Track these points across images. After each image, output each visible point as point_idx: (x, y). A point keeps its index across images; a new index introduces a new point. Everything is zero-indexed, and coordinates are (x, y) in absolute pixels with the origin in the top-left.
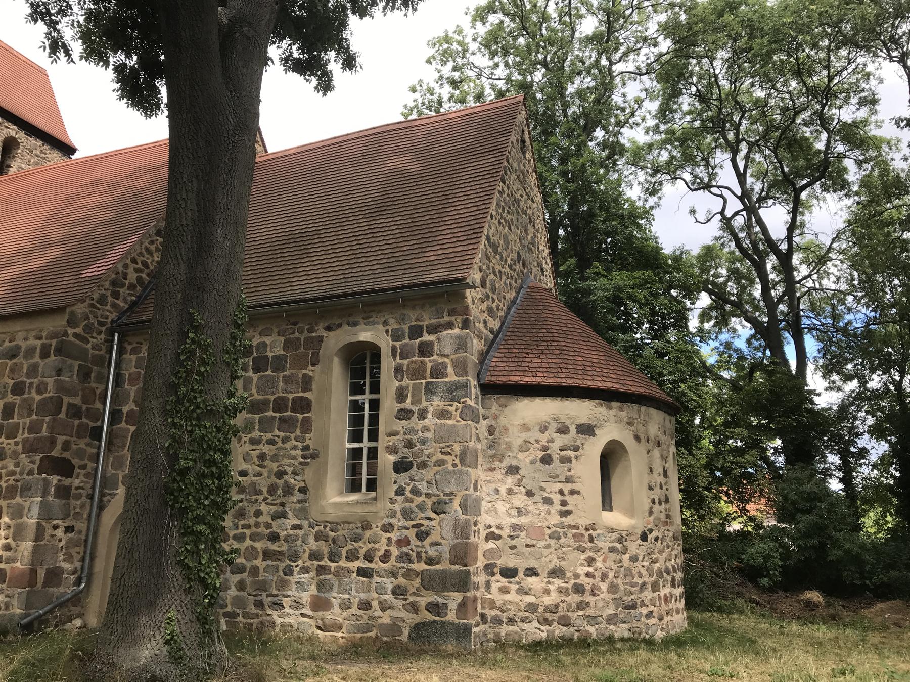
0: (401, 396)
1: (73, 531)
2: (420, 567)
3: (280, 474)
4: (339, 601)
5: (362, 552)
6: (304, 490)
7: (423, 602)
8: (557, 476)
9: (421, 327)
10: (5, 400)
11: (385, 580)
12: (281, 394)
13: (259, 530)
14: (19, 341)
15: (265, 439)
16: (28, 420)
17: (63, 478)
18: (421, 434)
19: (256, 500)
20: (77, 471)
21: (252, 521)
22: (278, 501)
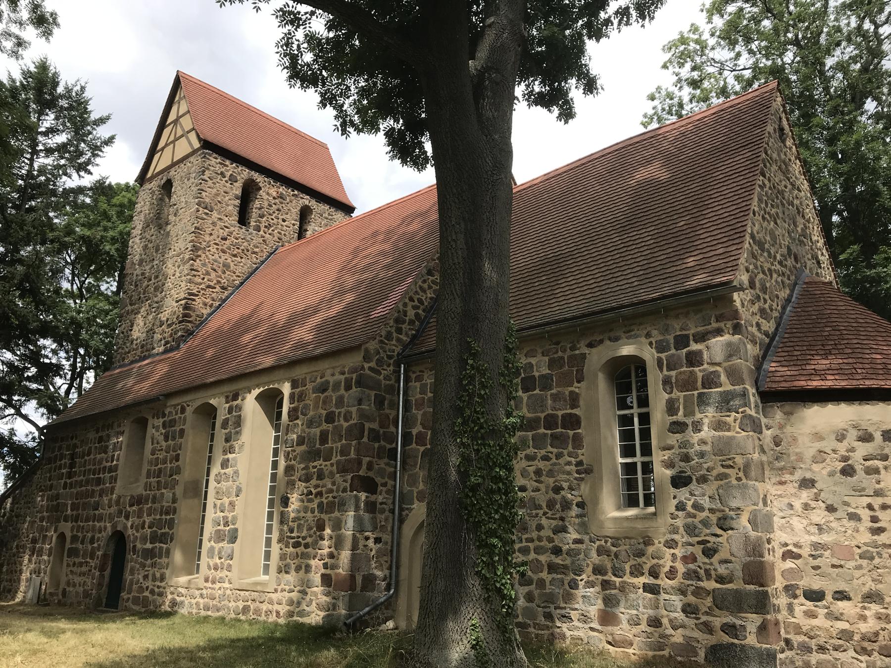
0: (671, 408)
1: (380, 542)
2: (711, 585)
3: (557, 489)
4: (627, 617)
5: (646, 568)
6: (581, 505)
7: (717, 622)
8: (864, 489)
9: (687, 336)
10: (321, 428)
11: (673, 597)
12: (551, 412)
13: (542, 544)
14: (328, 377)
15: (539, 456)
16: (339, 445)
17: (369, 495)
18: (697, 448)
19: (537, 515)
20: (380, 488)
21: (534, 535)
22: (558, 516)
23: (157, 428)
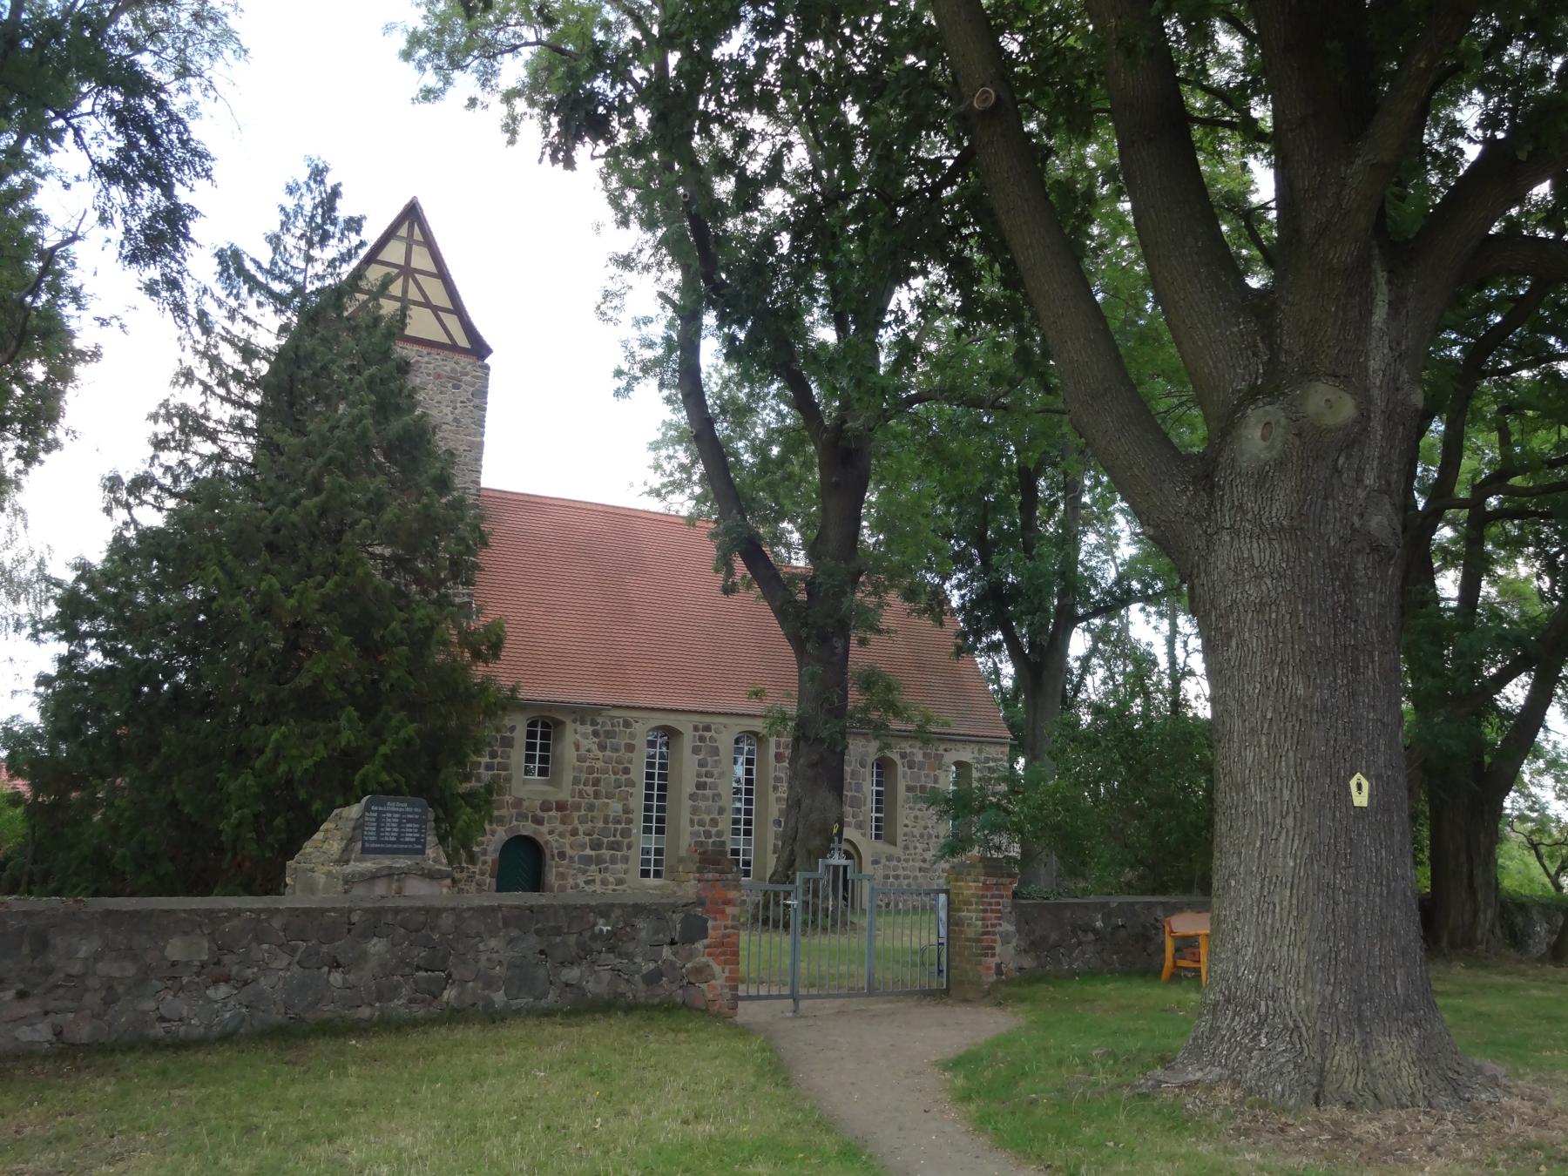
23: (585, 736)
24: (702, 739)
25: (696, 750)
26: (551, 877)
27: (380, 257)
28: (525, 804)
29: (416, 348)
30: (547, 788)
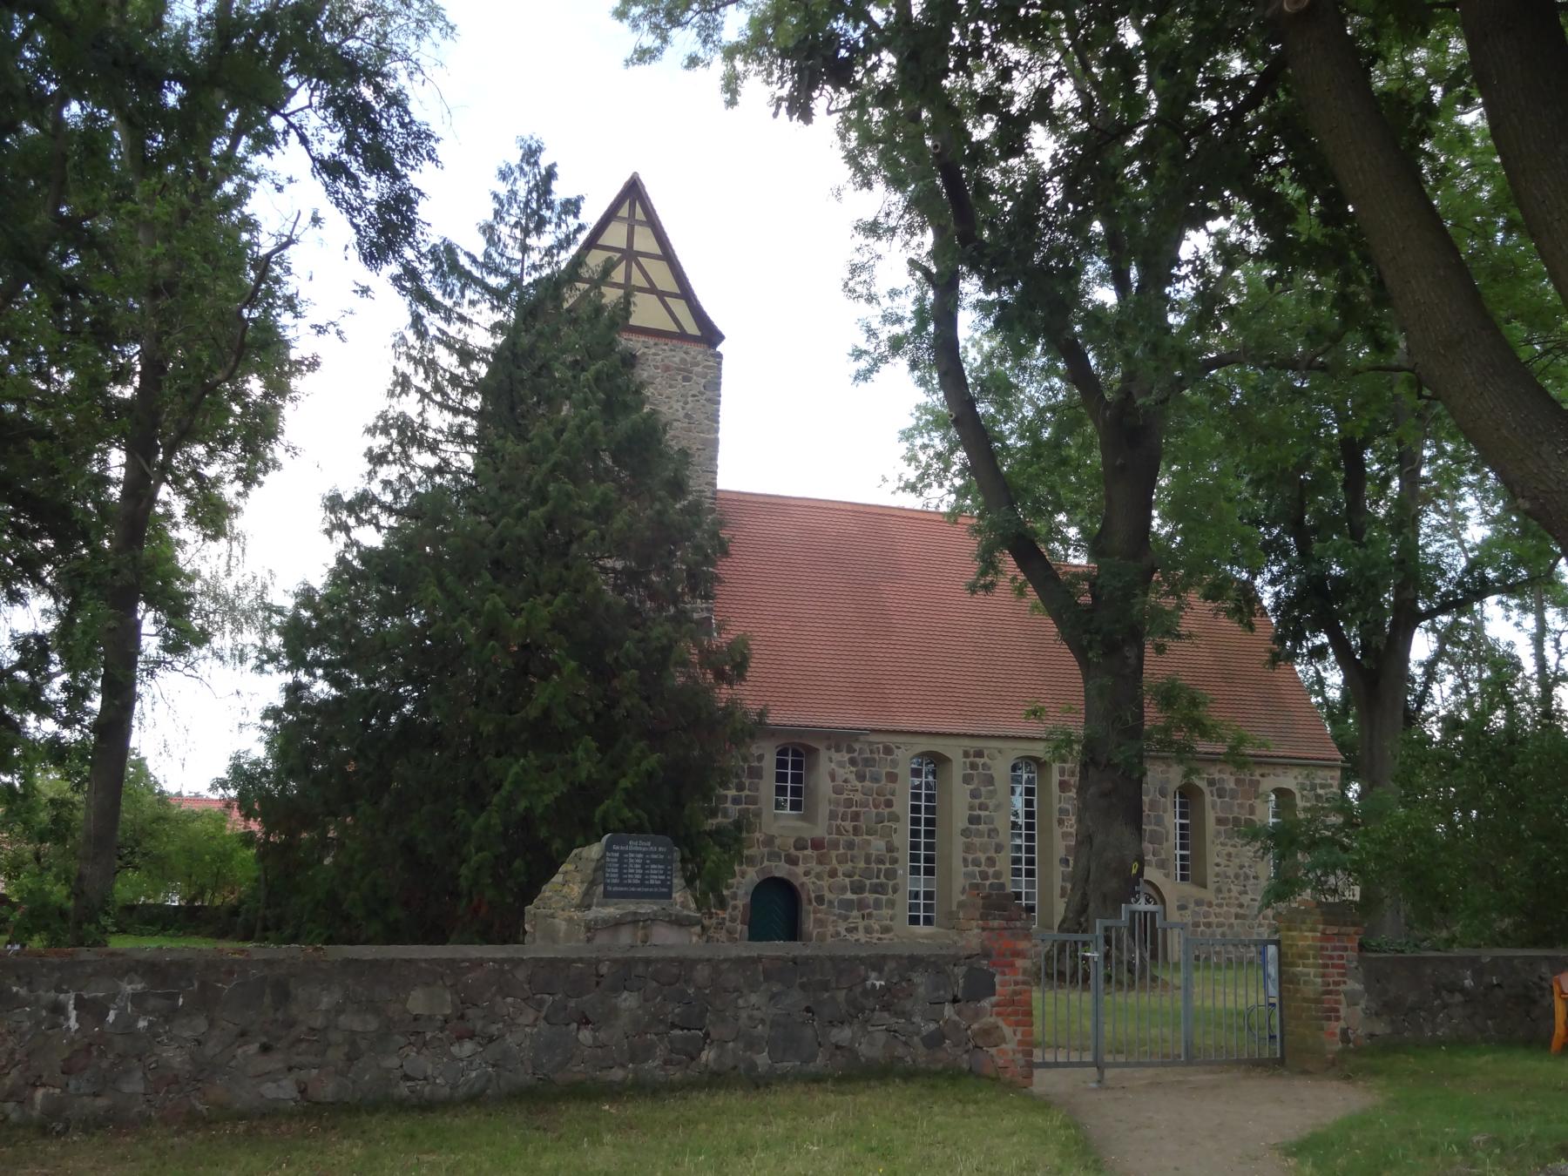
6: (1256, 878)
21: (1226, 895)
23: (841, 765)
24: (973, 766)
25: (967, 779)
26: (809, 924)
27: (601, 242)
28: (778, 842)
29: (642, 338)
30: (804, 825)
